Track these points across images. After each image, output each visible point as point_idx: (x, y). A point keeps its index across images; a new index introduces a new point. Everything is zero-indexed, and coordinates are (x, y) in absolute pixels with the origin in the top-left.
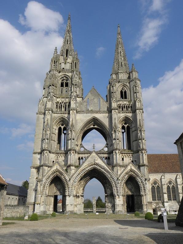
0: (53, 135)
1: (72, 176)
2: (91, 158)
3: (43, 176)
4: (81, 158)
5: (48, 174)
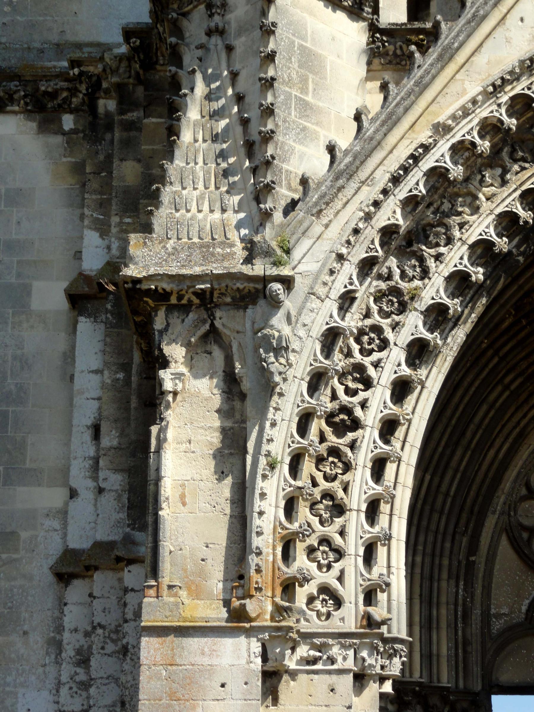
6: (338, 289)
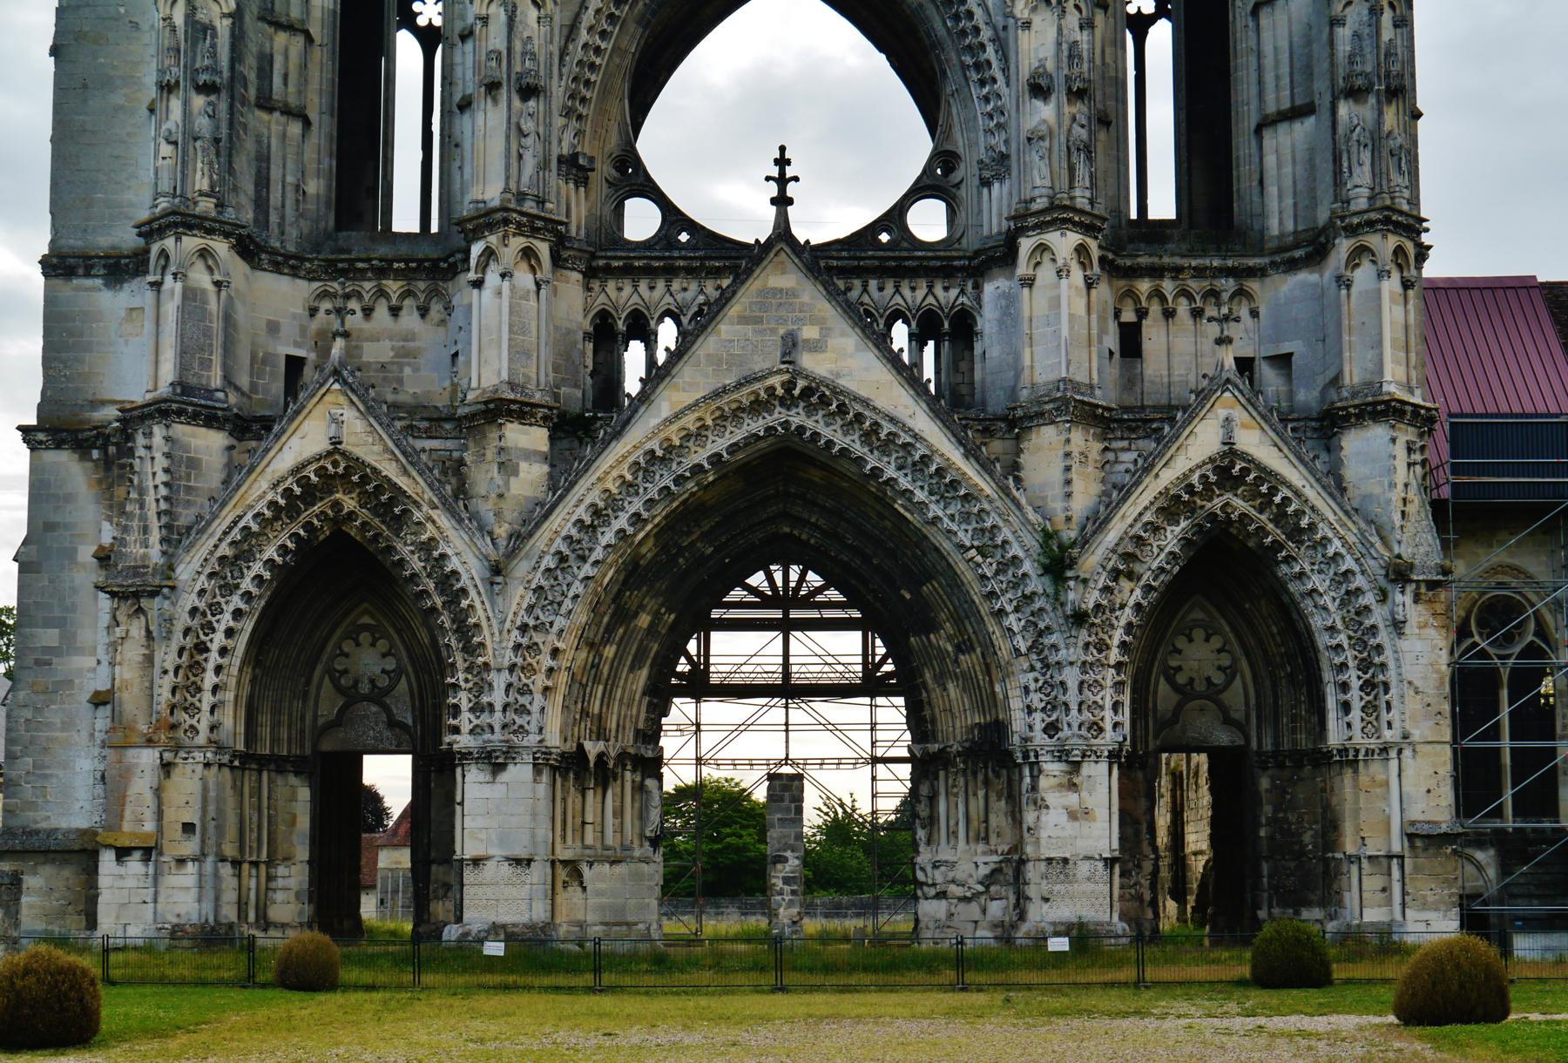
0: (281, 38)
1: (519, 538)
2: (743, 320)
3: (176, 537)
4: (621, 326)
5: (228, 516)
6: (197, 588)
